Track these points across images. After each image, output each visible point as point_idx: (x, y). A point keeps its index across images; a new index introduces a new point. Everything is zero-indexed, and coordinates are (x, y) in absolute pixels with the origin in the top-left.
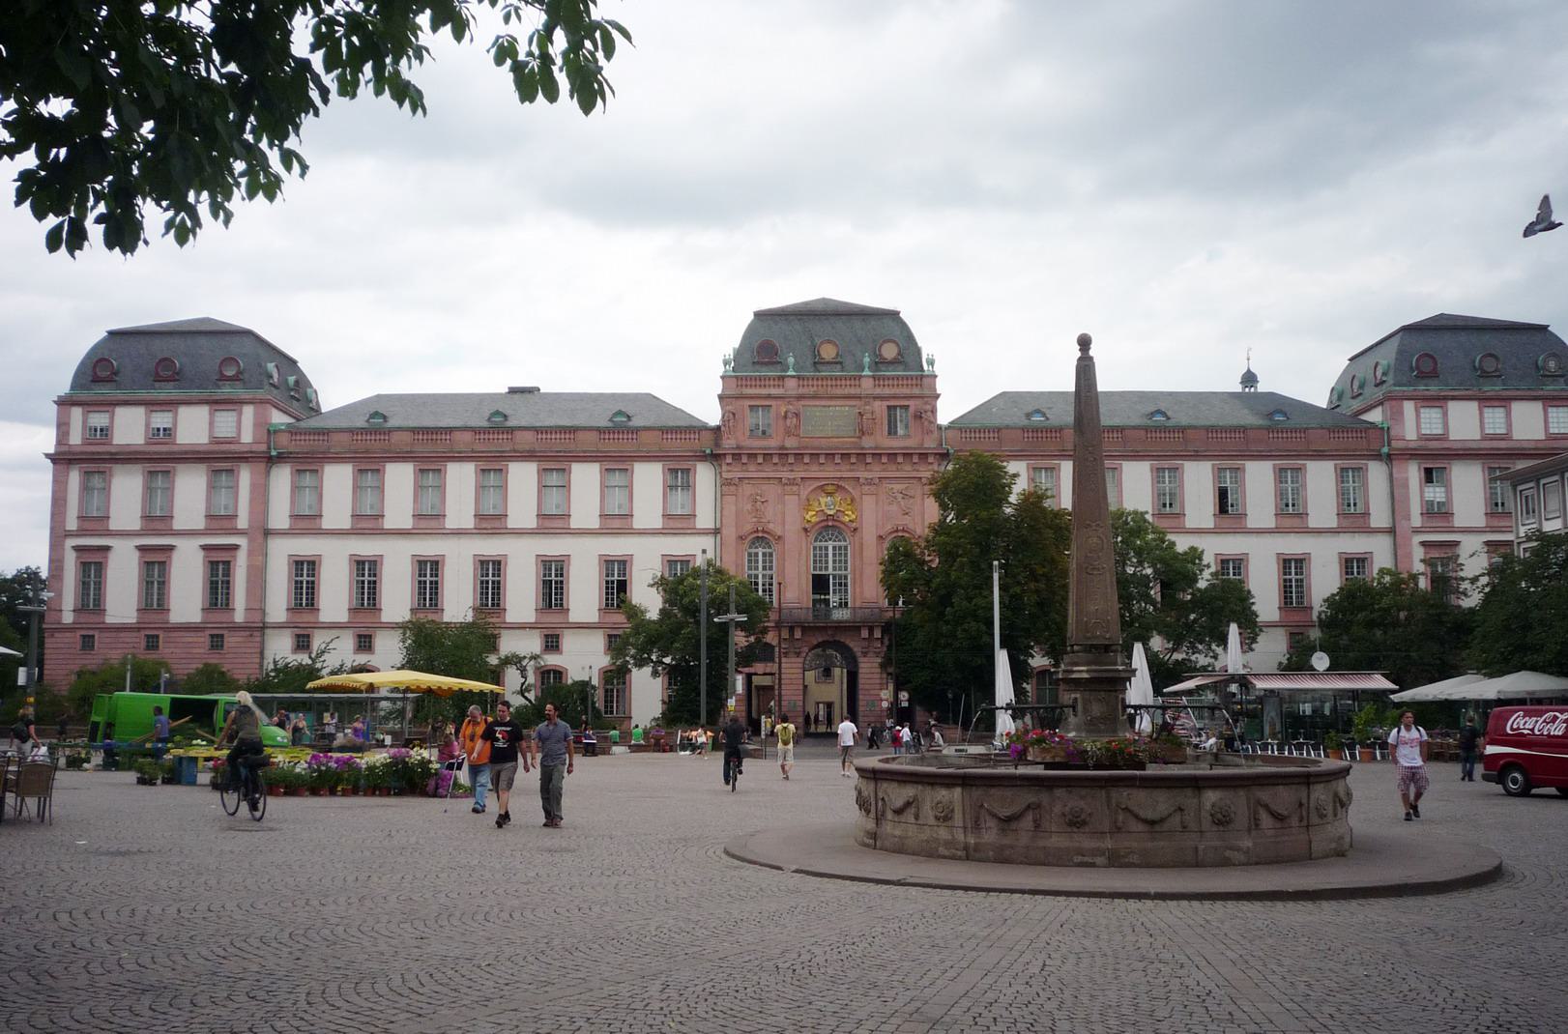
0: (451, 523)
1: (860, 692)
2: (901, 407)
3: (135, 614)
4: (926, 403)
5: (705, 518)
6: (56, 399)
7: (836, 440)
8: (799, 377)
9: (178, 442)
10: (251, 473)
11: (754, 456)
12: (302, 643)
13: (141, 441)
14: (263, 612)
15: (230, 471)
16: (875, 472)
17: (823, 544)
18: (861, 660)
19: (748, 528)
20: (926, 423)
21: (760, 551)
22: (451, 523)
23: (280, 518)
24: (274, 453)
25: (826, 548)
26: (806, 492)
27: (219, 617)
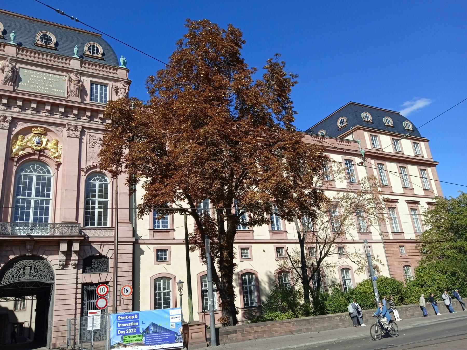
2: (102, 85)
18: (55, 273)
25: (31, 178)
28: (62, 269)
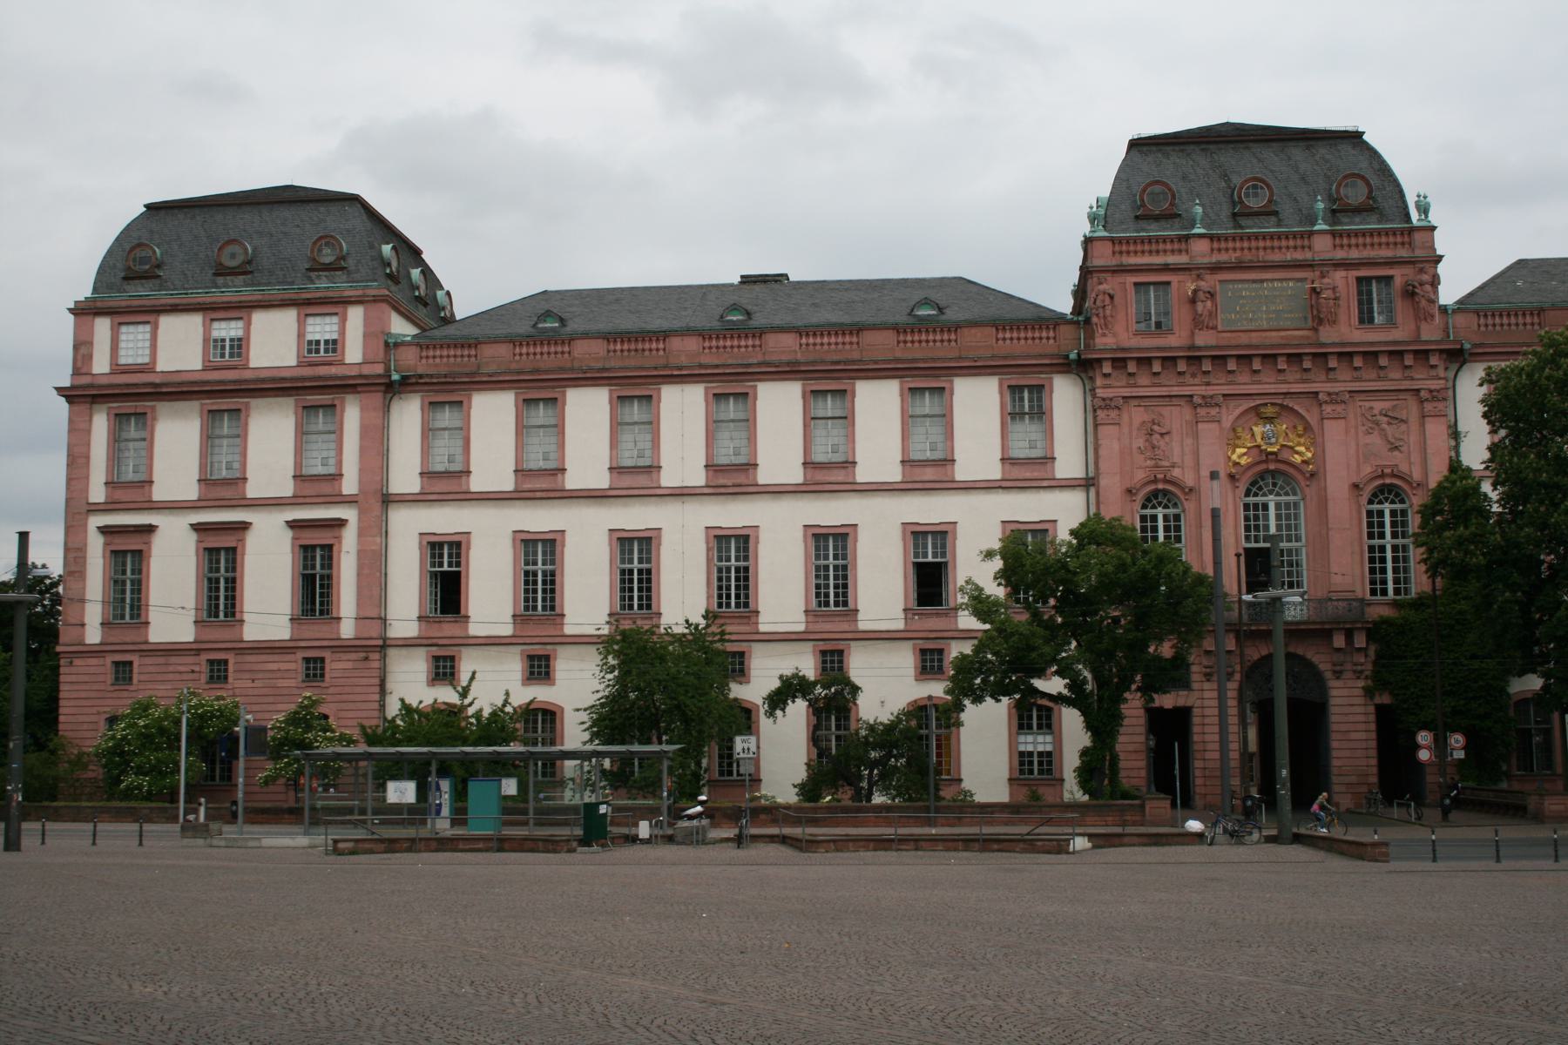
0: (668, 479)
1: (1334, 736)
2: (1379, 279)
3: (803, 618)
4: (1421, 271)
5: (1069, 461)
6: (72, 306)
7: (1274, 334)
8: (1211, 238)
9: (251, 366)
10: (362, 410)
11: (1148, 361)
12: (444, 670)
13: (291, 361)
14: (384, 620)
15: (553, 401)
16: (1343, 382)
17: (1259, 499)
19: (1140, 475)
20: (1423, 303)
21: (1387, 508)
22: (668, 479)
23: (405, 476)
24: (395, 377)
25: (1265, 507)
26: (1232, 418)
27: (316, 631)
28: (1338, 678)
